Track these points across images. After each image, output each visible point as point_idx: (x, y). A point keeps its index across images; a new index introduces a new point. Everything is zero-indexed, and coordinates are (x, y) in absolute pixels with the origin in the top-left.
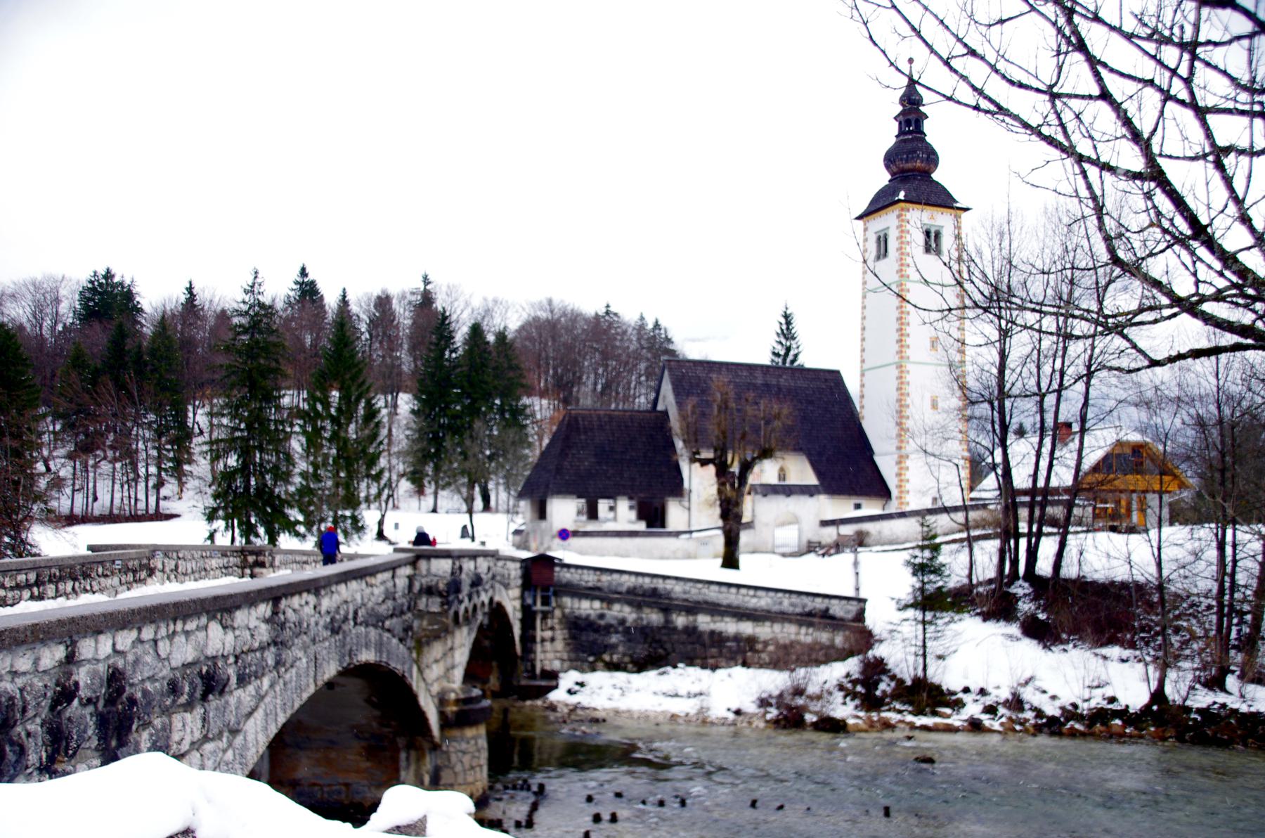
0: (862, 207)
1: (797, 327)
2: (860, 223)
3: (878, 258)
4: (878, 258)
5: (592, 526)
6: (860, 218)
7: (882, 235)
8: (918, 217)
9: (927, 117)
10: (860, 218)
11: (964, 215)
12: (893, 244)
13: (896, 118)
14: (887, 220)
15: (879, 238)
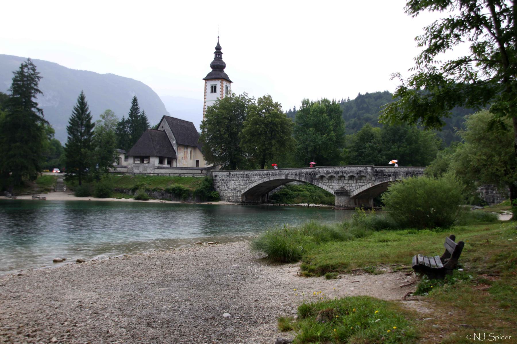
0: (205, 76)
1: (139, 102)
2: (204, 81)
3: (212, 92)
4: (212, 92)
5: (161, 166)
6: (204, 79)
7: (214, 86)
8: (225, 83)
9: (222, 53)
10: (204, 79)
11: (231, 83)
12: (218, 89)
13: (215, 53)
14: (218, 83)
15: (212, 87)
